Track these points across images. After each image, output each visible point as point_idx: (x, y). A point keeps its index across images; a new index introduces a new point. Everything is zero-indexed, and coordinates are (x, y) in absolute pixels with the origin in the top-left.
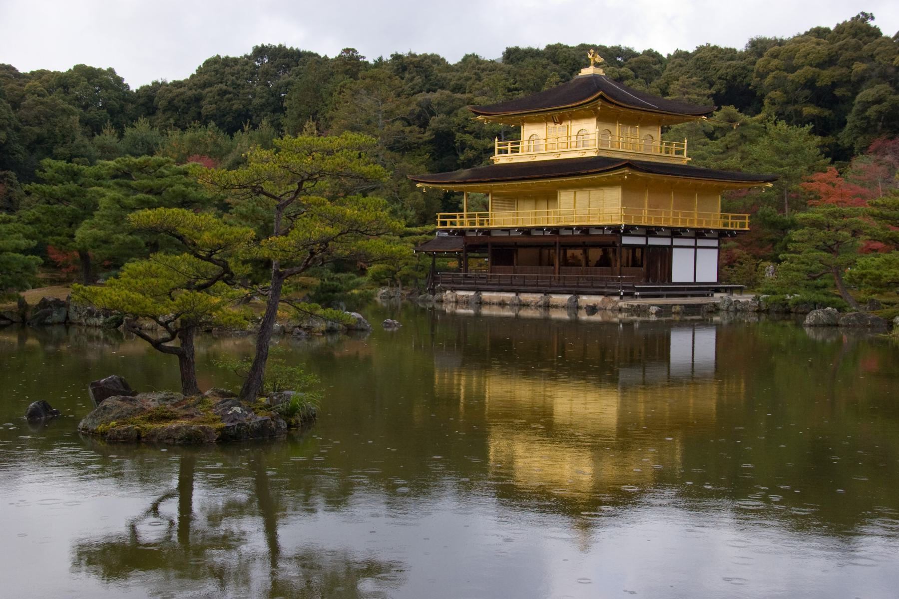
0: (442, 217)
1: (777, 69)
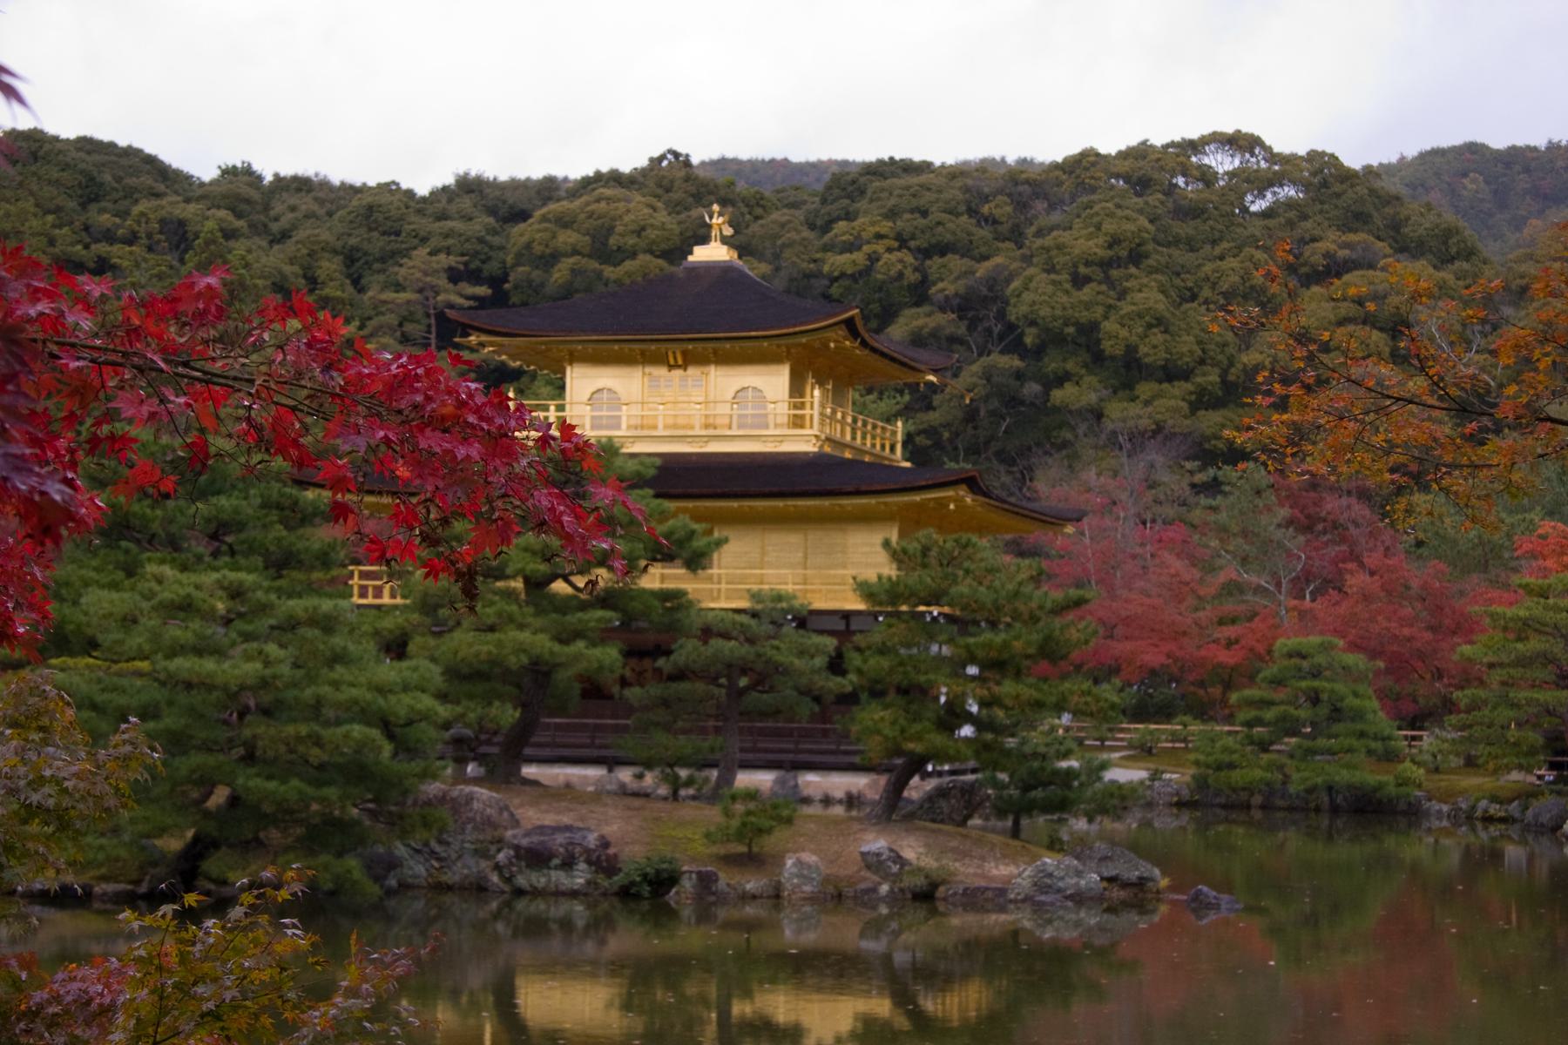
0: (364, 575)
1: (575, 252)
